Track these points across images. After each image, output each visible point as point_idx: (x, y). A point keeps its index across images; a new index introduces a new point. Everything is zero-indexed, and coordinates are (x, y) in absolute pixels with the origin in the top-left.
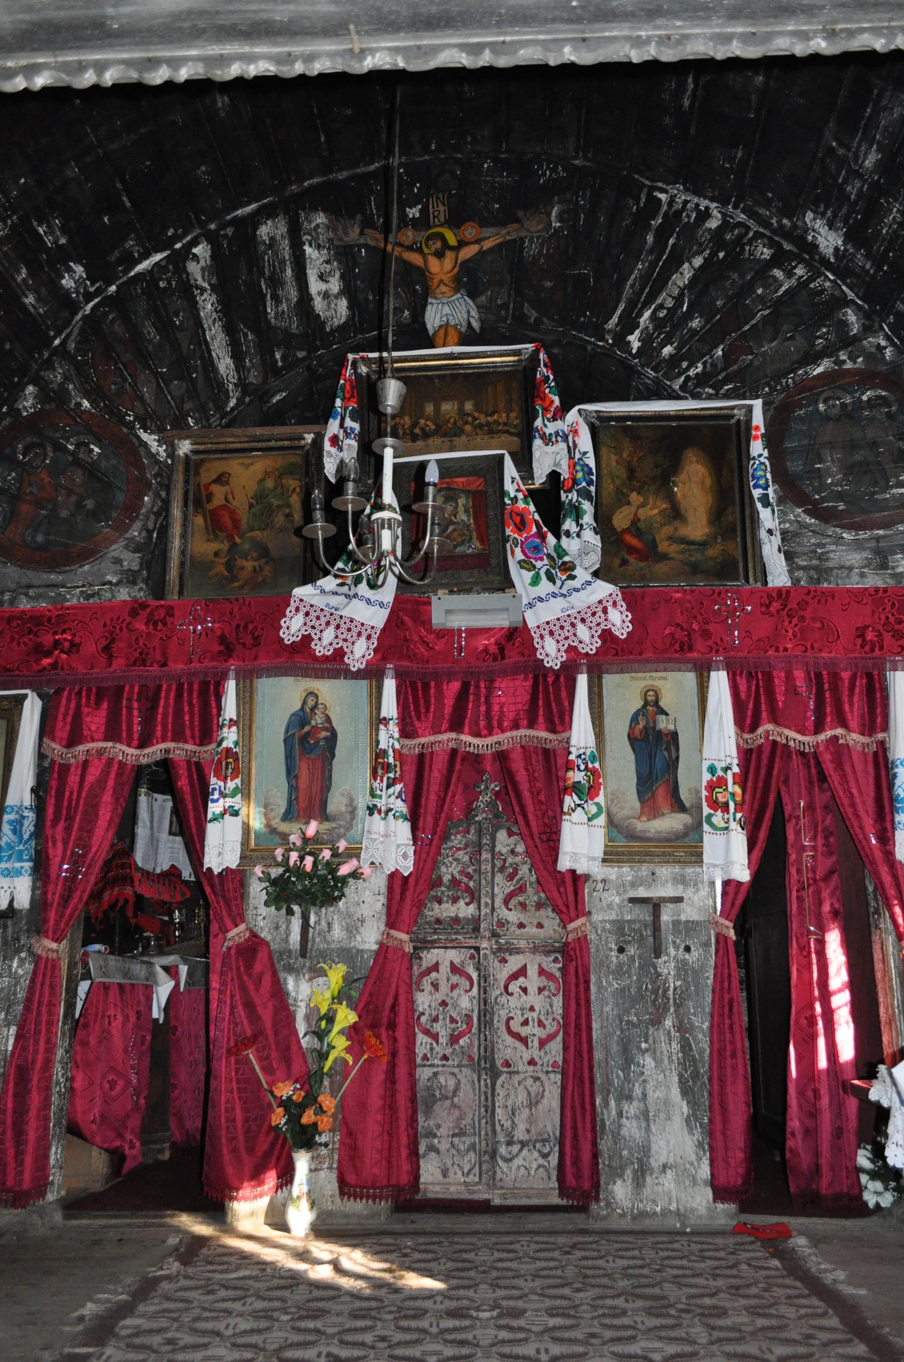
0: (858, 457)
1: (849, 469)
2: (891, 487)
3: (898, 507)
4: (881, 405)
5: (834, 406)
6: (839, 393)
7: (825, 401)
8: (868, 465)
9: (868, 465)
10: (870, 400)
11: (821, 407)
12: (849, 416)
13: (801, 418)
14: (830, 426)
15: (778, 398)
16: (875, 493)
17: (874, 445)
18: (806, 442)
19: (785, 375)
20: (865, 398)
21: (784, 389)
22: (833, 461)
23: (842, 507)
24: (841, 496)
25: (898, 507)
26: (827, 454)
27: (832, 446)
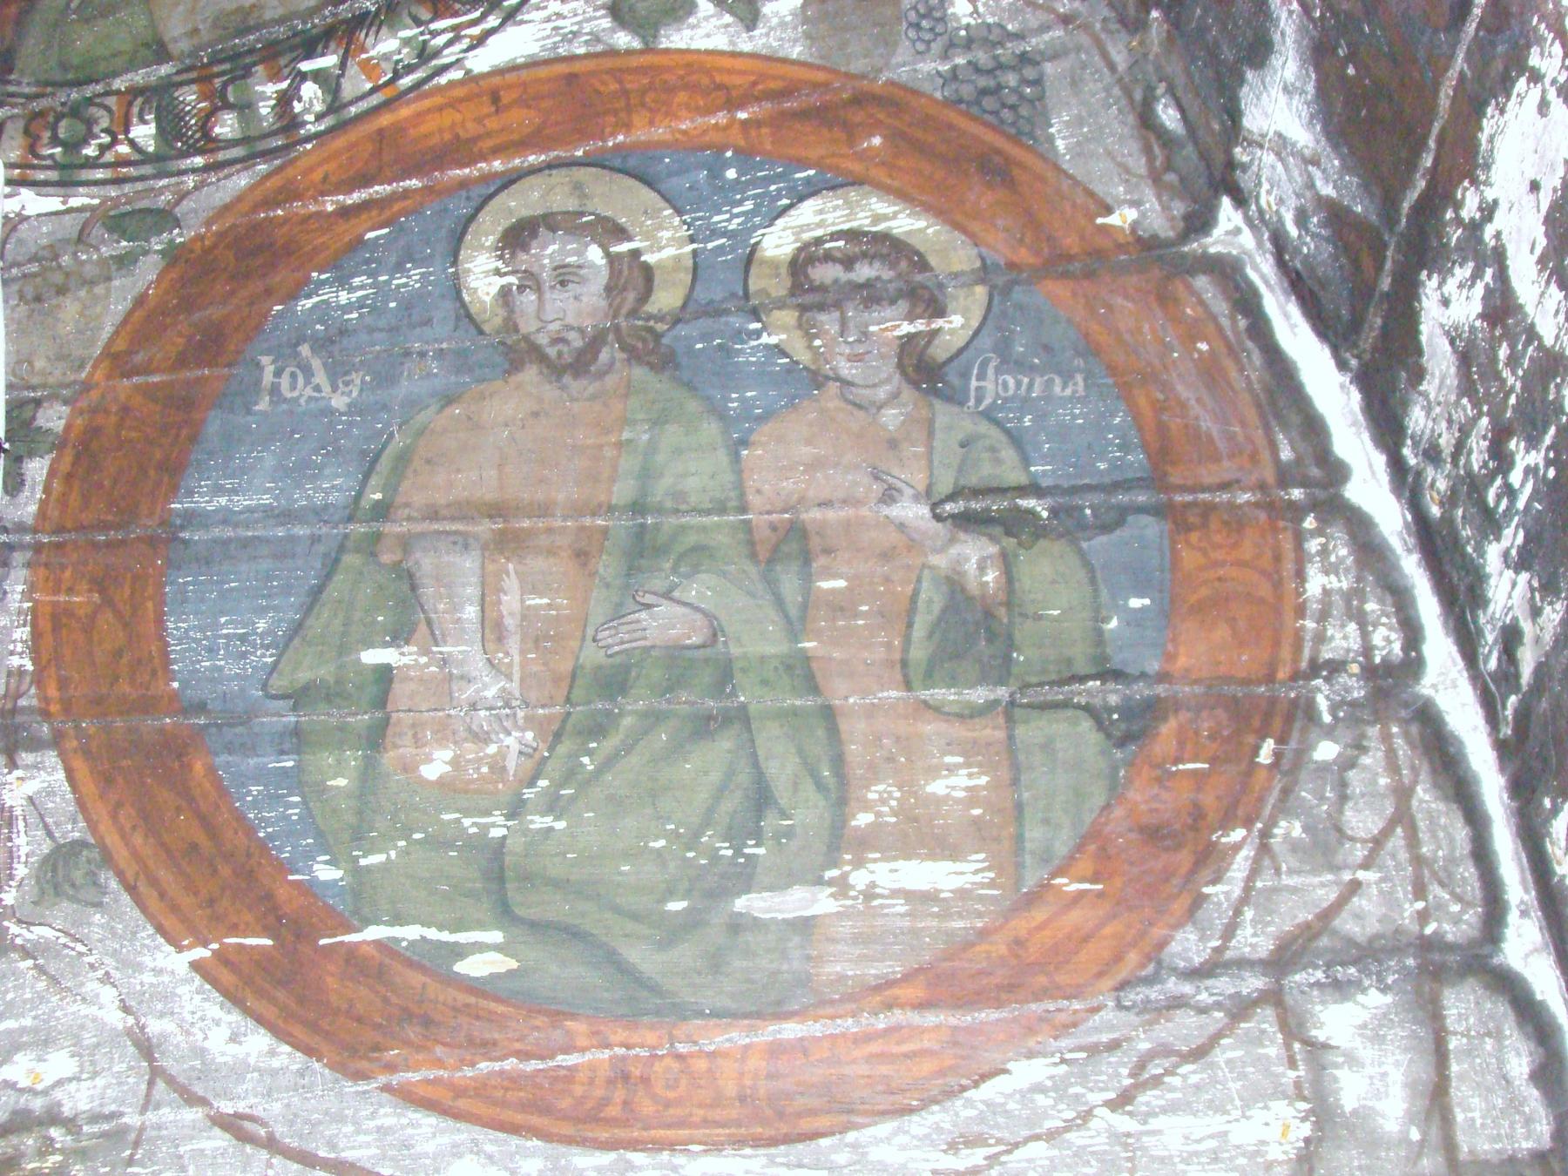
0: (664, 623)
1: (591, 702)
2: (864, 845)
3: (882, 993)
4: (871, 295)
5: (565, 276)
6: (616, 197)
7: (517, 238)
8: (725, 674)
9: (725, 674)
10: (802, 262)
11: (483, 275)
12: (652, 350)
13: (334, 340)
14: (512, 403)
15: (209, 197)
16: (745, 877)
17: (792, 545)
18: (333, 487)
19: (286, 50)
20: (778, 242)
21: (252, 147)
22: (492, 629)
23: (484, 962)
24: (497, 884)
25: (882, 993)
26: (457, 582)
27: (506, 530)
